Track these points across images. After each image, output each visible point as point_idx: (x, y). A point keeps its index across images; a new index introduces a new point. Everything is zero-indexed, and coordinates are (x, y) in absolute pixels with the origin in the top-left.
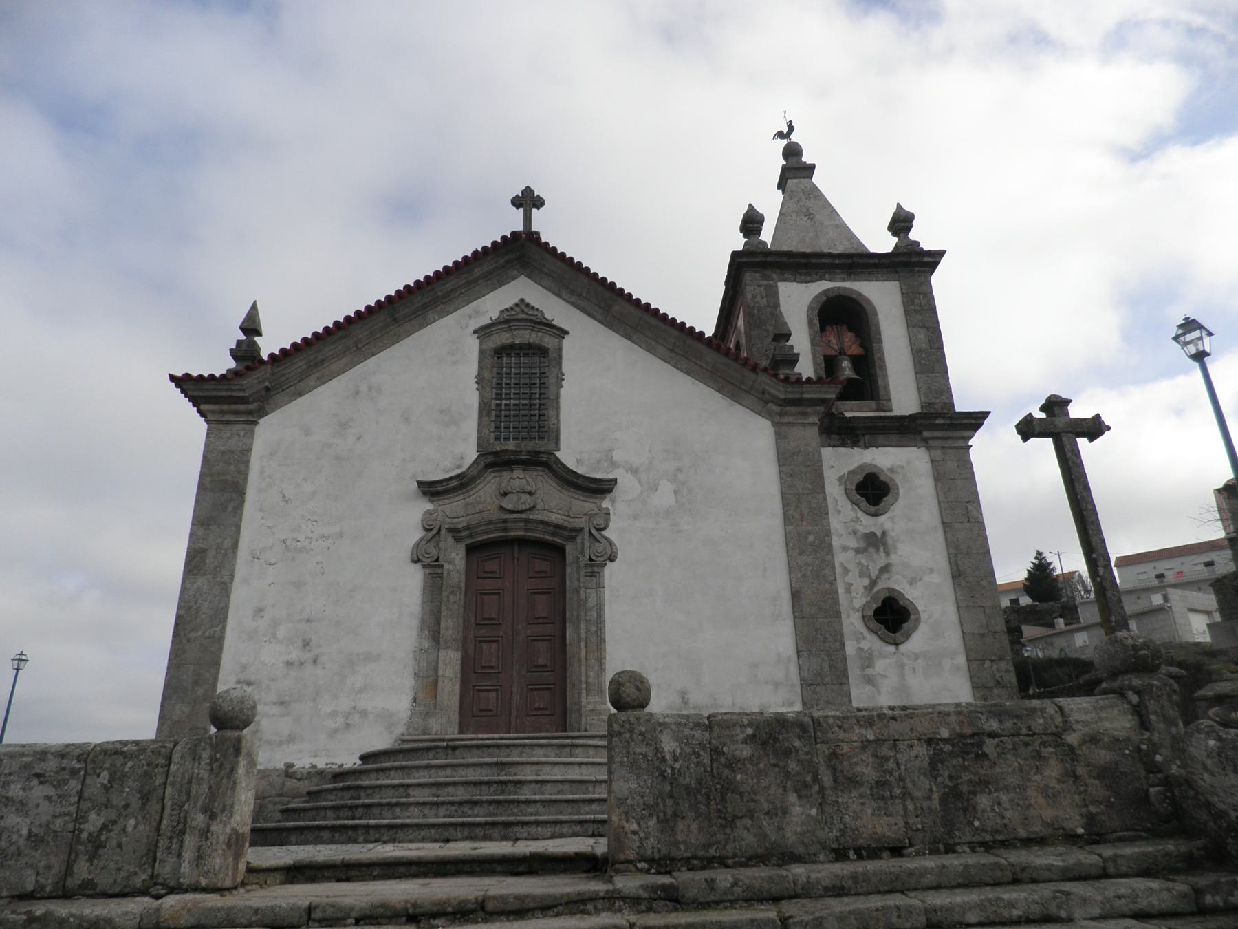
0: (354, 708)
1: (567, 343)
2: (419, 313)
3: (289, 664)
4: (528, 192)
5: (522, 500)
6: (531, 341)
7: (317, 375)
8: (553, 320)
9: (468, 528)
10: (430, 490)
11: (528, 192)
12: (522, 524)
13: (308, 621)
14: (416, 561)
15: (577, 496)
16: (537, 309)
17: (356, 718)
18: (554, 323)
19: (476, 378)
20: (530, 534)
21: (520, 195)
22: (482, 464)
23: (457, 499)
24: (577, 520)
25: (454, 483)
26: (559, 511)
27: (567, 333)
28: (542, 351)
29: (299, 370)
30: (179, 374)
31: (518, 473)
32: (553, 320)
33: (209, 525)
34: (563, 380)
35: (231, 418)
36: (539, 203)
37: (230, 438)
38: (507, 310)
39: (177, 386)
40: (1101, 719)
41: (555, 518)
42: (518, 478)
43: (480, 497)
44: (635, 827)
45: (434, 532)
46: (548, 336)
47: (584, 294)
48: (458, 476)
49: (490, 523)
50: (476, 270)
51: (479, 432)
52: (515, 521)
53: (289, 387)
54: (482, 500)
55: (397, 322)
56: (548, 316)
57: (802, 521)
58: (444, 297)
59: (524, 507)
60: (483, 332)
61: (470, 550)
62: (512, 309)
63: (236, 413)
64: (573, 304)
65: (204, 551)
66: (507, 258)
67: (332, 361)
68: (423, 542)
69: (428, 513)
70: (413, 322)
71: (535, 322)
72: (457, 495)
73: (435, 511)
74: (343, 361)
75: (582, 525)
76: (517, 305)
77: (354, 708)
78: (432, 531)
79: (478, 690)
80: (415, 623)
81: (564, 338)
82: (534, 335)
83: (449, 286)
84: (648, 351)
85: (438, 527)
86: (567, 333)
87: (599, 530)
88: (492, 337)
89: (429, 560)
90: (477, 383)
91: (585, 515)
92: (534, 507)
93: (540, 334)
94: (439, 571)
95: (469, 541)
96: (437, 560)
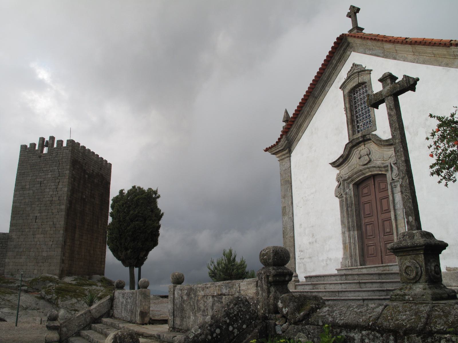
0: (328, 258)
2: (323, 90)
3: (310, 243)
4: (352, 8)
5: (365, 159)
7: (301, 131)
9: (349, 178)
10: (336, 164)
11: (352, 8)
12: (368, 170)
13: (312, 227)
14: (337, 196)
15: (385, 150)
17: (329, 262)
18: (366, 68)
20: (373, 173)
23: (345, 166)
24: (387, 161)
25: (341, 160)
26: (380, 160)
27: (371, 70)
28: (364, 83)
29: (295, 132)
30: (265, 149)
33: (285, 197)
35: (283, 157)
36: (358, 10)
37: (285, 164)
40: (248, 289)
41: (378, 163)
42: (362, 149)
43: (352, 162)
46: (365, 76)
48: (341, 157)
49: (356, 173)
50: (334, 61)
52: (365, 169)
53: (295, 139)
54: (353, 163)
55: (317, 98)
58: (328, 79)
59: (366, 162)
60: (343, 87)
61: (357, 185)
62: (351, 70)
63: (284, 155)
64: (371, 54)
65: (285, 207)
66: (342, 49)
69: (338, 175)
70: (322, 95)
71: (359, 72)
72: (345, 164)
73: (340, 173)
75: (388, 164)
76: (352, 68)
77: (328, 258)
78: (342, 182)
79: (368, 246)
80: (339, 222)
81: (370, 73)
83: (327, 74)
84: (404, 61)
86: (371, 70)
88: (347, 87)
89: (339, 195)
93: (362, 76)
96: (341, 195)
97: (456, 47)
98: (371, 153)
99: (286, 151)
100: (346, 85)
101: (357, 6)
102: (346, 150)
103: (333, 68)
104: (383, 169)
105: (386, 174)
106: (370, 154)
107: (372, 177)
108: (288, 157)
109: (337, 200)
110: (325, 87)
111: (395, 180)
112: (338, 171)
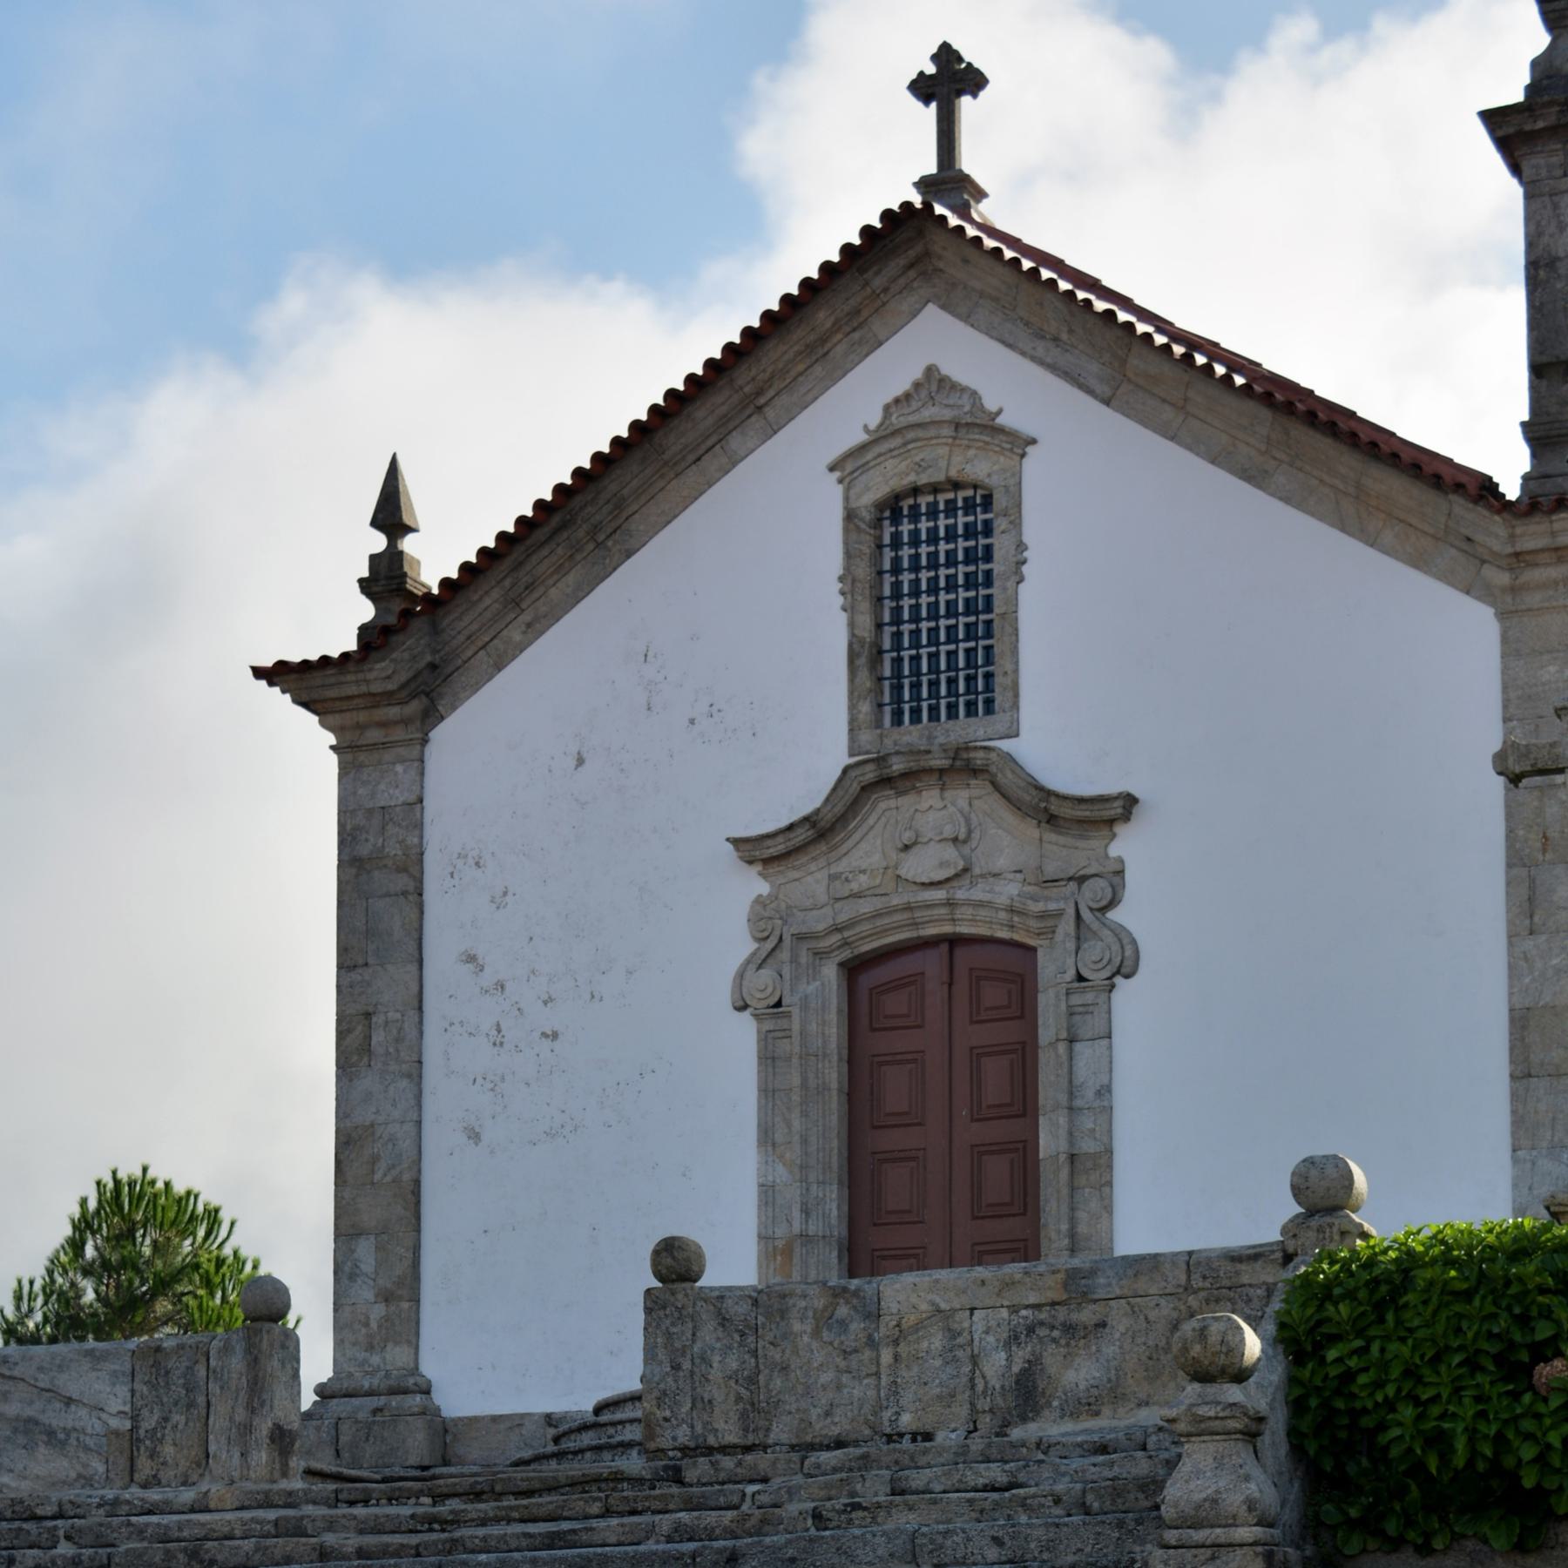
1: (1034, 467)
4: (947, 54)
6: (953, 473)
8: (1000, 412)
11: (947, 54)
12: (943, 911)
16: (964, 389)
18: (1000, 420)
19: (841, 579)
21: (931, 69)
22: (855, 788)
25: (802, 835)
31: (930, 797)
32: (1000, 412)
34: (1024, 562)
36: (974, 81)
38: (897, 401)
39: (271, 684)
44: (668, 1413)
45: (770, 945)
47: (1064, 336)
50: (821, 315)
51: (852, 707)
56: (991, 404)
57: (1544, 851)
60: (848, 466)
62: (907, 396)
67: (551, 582)
68: (753, 967)
69: (759, 901)
73: (773, 897)
74: (571, 579)
81: (1023, 456)
82: (957, 459)
85: (777, 933)
86: (1033, 442)
87: (1104, 909)
89: (765, 1003)
90: (843, 593)
91: (1070, 879)
92: (966, 870)
94: (783, 1023)
95: (846, 954)
96: (778, 1004)
97: (1471, 506)
98: (976, 835)
99: (415, 707)
100: (867, 463)
101: (971, 54)
102: (840, 792)
103: (807, 346)
104: (1033, 924)
105: (1033, 950)
106: (965, 842)
107: (945, 947)
108: (408, 742)
109: (744, 1033)
110: (731, 426)
111: (1090, 984)
112: (763, 888)
